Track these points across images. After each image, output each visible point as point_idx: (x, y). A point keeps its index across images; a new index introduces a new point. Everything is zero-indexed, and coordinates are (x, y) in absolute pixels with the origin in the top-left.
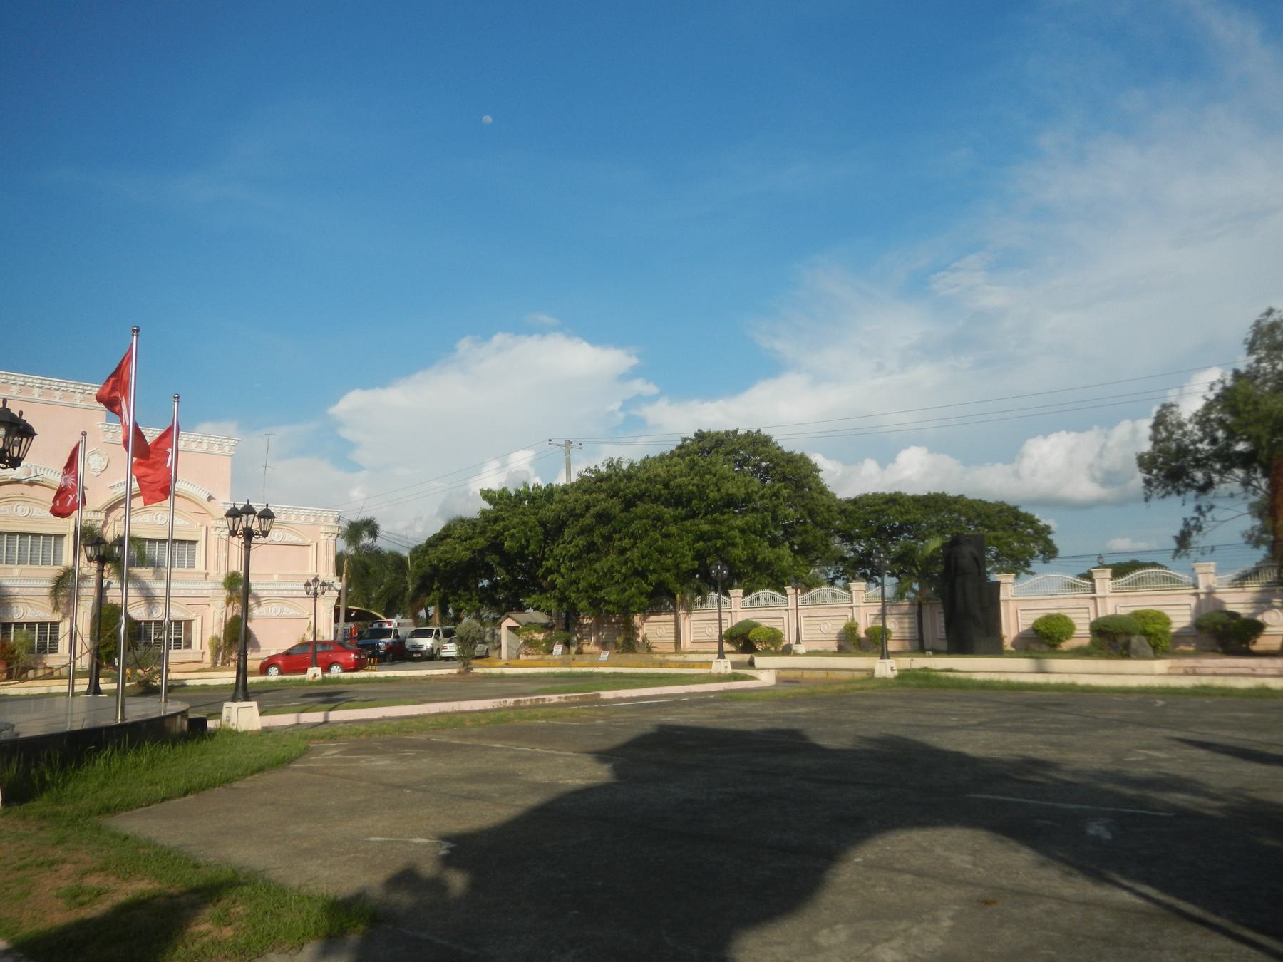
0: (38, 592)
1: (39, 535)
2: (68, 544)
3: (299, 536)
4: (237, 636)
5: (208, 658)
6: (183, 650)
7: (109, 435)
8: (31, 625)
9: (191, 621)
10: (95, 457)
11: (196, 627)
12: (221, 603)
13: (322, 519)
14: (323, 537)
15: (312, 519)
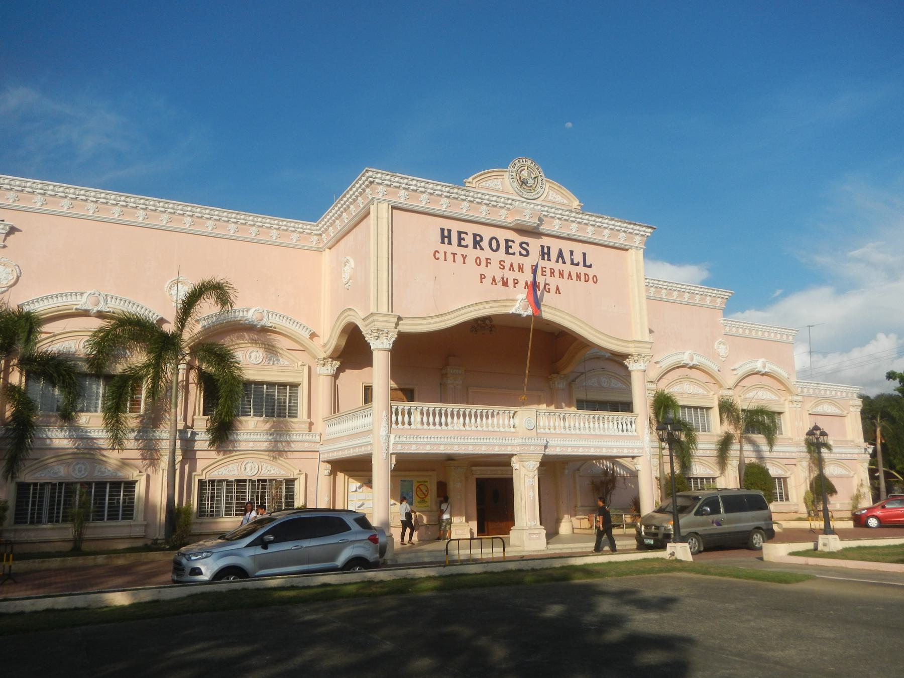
0: (708, 453)
1: (696, 408)
2: (715, 413)
3: (838, 408)
4: (822, 488)
5: (803, 509)
6: (785, 503)
7: (727, 329)
8: (702, 479)
9: (785, 479)
10: (722, 346)
11: (791, 483)
12: (805, 464)
13: (850, 394)
14: (852, 409)
15: (844, 394)
